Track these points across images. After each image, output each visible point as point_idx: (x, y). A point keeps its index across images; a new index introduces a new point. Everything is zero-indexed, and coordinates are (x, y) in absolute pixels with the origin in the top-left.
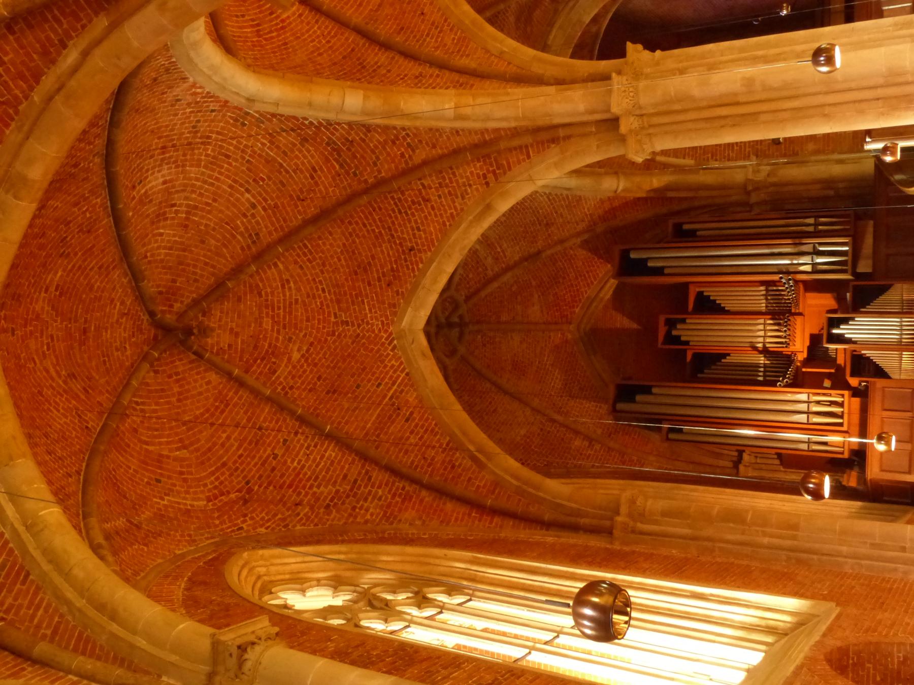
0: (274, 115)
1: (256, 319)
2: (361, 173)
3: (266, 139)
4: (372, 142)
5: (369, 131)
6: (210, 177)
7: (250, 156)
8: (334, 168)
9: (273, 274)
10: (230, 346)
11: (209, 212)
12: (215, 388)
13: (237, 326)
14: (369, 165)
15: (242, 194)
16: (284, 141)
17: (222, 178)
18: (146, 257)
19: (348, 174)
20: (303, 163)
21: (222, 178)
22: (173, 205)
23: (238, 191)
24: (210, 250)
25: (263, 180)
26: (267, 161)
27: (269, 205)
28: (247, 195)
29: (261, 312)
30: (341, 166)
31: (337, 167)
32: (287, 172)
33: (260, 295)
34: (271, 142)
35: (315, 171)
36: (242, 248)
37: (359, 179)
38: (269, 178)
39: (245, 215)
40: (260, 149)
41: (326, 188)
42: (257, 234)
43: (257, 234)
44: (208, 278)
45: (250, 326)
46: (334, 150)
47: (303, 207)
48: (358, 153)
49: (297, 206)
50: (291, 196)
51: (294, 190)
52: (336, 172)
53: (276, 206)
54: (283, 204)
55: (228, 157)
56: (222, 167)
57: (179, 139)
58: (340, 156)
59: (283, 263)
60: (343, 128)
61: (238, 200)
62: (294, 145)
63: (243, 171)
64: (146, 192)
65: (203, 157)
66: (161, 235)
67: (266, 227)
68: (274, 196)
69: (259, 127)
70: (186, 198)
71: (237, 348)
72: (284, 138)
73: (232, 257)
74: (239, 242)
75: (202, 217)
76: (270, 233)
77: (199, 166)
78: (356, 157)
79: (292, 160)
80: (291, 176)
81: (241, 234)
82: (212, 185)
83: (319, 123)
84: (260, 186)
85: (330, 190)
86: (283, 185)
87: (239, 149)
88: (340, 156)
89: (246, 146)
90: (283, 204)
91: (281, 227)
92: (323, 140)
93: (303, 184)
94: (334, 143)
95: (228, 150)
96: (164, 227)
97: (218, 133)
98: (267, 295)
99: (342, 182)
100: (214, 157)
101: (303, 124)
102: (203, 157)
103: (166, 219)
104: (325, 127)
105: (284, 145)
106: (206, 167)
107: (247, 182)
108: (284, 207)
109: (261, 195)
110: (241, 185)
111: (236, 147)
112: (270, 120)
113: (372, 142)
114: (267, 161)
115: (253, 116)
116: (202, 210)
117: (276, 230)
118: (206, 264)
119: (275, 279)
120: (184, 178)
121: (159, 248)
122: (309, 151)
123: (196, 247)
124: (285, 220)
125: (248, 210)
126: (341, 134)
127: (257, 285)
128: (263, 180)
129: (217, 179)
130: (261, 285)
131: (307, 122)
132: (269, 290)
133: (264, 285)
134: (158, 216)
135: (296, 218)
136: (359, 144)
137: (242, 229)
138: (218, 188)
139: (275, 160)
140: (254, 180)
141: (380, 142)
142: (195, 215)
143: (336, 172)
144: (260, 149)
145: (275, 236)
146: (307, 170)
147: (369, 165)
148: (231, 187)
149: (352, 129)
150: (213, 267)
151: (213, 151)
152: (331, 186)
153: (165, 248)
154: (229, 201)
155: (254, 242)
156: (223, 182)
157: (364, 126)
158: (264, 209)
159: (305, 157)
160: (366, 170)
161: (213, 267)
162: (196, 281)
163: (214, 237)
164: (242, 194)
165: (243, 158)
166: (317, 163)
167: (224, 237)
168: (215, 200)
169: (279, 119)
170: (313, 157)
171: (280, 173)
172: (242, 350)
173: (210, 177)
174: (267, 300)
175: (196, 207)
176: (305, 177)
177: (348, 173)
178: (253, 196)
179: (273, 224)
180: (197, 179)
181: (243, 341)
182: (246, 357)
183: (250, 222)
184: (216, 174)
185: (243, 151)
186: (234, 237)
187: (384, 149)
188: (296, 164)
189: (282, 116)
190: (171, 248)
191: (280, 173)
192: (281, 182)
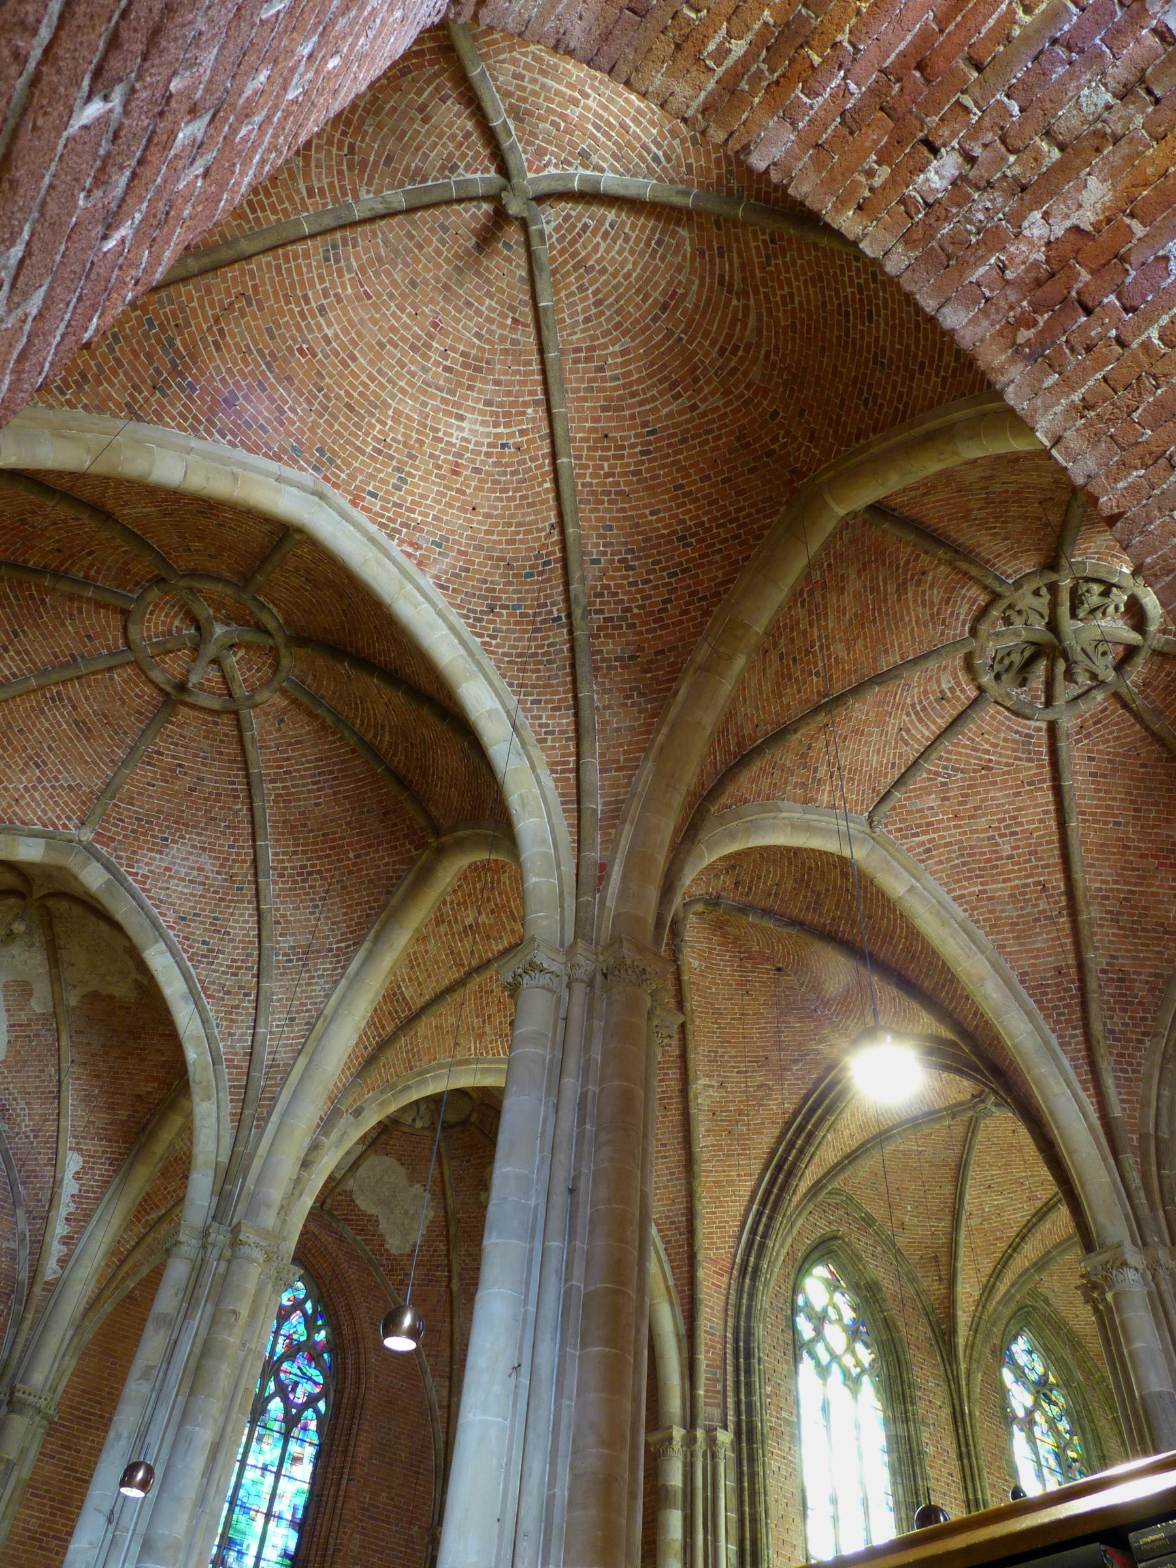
0: (277, 458)
1: (377, 113)
2: (141, 325)
3: (288, 418)
4: (120, 381)
5: (128, 405)
6: (382, 386)
7: (316, 397)
8: (184, 342)
9: (319, 179)
10: (443, 100)
11: (393, 329)
12: (515, 62)
13: (412, 120)
14: (125, 337)
15: (336, 335)
16: (262, 408)
17: (364, 377)
18: (515, 321)
19: (161, 325)
20: (235, 364)
21: (364, 377)
22: (447, 369)
23: (342, 345)
24: (407, 265)
25: (300, 350)
26: (289, 379)
27: (298, 304)
28: (330, 333)
29: (362, 120)
30: (171, 341)
31: (178, 342)
32: (263, 356)
33: (351, 147)
34: (283, 412)
35: (216, 343)
36: (355, 245)
37: (145, 312)
38: (290, 349)
39: (339, 298)
40: (300, 404)
41: (202, 307)
42: (327, 259)
43: (327, 259)
44: (425, 222)
45: (394, 109)
46: (181, 374)
47: (244, 284)
48: (142, 364)
49: (255, 287)
50: (261, 309)
51: (255, 318)
52: (181, 333)
53: (288, 303)
54: (277, 301)
55: (349, 407)
56: (361, 394)
57: (428, 472)
58: (174, 365)
59: (298, 192)
60: (173, 419)
61: (345, 331)
62: (246, 397)
63: (331, 376)
64: (496, 425)
65: (390, 423)
66: (478, 335)
67: (309, 266)
68: (287, 318)
69: (298, 441)
70: (425, 370)
71: (437, 90)
72: (260, 413)
73: (375, 236)
74: (357, 257)
75: (406, 327)
76: (306, 255)
77: (396, 411)
78: (147, 355)
79: (252, 372)
80: (256, 344)
81: (350, 270)
82: (380, 371)
83: (211, 434)
84: (306, 341)
85: (195, 304)
86: (269, 330)
87: (331, 414)
88: (173, 362)
89: (321, 416)
90: (277, 301)
91: (287, 261)
92: (204, 402)
93: (238, 325)
94: (183, 389)
95: (349, 419)
96: (473, 345)
97: (363, 453)
98: (341, 142)
99: (173, 311)
100: (372, 415)
101: (235, 436)
102: (390, 423)
103: (464, 354)
104: (200, 423)
105: (262, 403)
106: (388, 406)
107: (326, 356)
108: (275, 292)
109: (308, 325)
110: (337, 354)
111: (336, 419)
112: (285, 451)
113: (120, 381)
114: (289, 379)
115: (309, 463)
116: (404, 339)
117: (296, 258)
118: (420, 247)
119: (318, 166)
120: (424, 404)
121: (490, 320)
122: (223, 380)
123: (426, 282)
124: (278, 268)
125: (333, 308)
126: (173, 405)
127: (351, 168)
128: (300, 350)
129: (372, 378)
130: (345, 167)
131: (229, 437)
132: (334, 150)
133: (340, 163)
134: (478, 369)
135: (260, 268)
136: (144, 381)
137: (347, 276)
138: (371, 363)
139: (276, 377)
140: (314, 355)
141: (108, 380)
142: (416, 336)
143: (181, 333)
144: (300, 404)
145: (299, 247)
146: (227, 346)
147: (125, 337)
148: (354, 358)
149: (155, 412)
150: (410, 237)
151: (373, 427)
152: (193, 310)
153: (478, 312)
154: (358, 333)
155: (335, 247)
156: (363, 369)
157: (139, 419)
158: (307, 302)
159: (229, 370)
160: (131, 328)
161: (410, 237)
162: (445, 229)
163: (394, 283)
164: (336, 335)
165: (326, 396)
166: (212, 359)
167: (376, 274)
168: (382, 346)
169: (271, 449)
170: (217, 368)
171: (272, 354)
172: (428, 82)
173: (382, 386)
174: (344, 133)
175: (413, 347)
176: (233, 336)
177: (163, 329)
178: (320, 329)
179: (299, 267)
180: (403, 391)
181: (419, 93)
182: (430, 70)
183: (333, 285)
184: (372, 387)
185: (326, 408)
186: (362, 269)
187: (98, 365)
188: (247, 364)
189: (266, 455)
190: (469, 304)
191: (272, 354)
192: (272, 337)
